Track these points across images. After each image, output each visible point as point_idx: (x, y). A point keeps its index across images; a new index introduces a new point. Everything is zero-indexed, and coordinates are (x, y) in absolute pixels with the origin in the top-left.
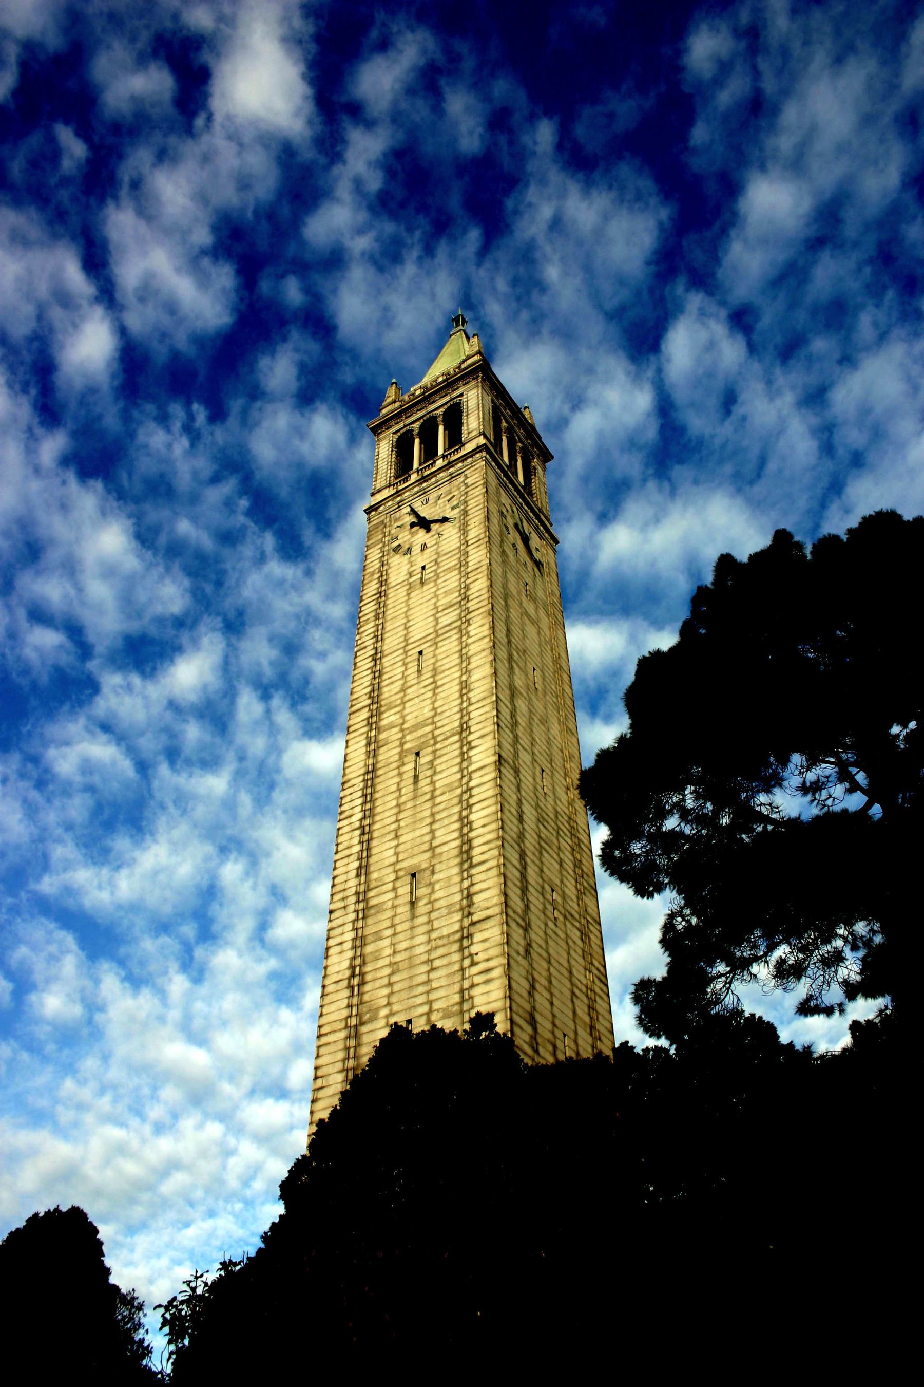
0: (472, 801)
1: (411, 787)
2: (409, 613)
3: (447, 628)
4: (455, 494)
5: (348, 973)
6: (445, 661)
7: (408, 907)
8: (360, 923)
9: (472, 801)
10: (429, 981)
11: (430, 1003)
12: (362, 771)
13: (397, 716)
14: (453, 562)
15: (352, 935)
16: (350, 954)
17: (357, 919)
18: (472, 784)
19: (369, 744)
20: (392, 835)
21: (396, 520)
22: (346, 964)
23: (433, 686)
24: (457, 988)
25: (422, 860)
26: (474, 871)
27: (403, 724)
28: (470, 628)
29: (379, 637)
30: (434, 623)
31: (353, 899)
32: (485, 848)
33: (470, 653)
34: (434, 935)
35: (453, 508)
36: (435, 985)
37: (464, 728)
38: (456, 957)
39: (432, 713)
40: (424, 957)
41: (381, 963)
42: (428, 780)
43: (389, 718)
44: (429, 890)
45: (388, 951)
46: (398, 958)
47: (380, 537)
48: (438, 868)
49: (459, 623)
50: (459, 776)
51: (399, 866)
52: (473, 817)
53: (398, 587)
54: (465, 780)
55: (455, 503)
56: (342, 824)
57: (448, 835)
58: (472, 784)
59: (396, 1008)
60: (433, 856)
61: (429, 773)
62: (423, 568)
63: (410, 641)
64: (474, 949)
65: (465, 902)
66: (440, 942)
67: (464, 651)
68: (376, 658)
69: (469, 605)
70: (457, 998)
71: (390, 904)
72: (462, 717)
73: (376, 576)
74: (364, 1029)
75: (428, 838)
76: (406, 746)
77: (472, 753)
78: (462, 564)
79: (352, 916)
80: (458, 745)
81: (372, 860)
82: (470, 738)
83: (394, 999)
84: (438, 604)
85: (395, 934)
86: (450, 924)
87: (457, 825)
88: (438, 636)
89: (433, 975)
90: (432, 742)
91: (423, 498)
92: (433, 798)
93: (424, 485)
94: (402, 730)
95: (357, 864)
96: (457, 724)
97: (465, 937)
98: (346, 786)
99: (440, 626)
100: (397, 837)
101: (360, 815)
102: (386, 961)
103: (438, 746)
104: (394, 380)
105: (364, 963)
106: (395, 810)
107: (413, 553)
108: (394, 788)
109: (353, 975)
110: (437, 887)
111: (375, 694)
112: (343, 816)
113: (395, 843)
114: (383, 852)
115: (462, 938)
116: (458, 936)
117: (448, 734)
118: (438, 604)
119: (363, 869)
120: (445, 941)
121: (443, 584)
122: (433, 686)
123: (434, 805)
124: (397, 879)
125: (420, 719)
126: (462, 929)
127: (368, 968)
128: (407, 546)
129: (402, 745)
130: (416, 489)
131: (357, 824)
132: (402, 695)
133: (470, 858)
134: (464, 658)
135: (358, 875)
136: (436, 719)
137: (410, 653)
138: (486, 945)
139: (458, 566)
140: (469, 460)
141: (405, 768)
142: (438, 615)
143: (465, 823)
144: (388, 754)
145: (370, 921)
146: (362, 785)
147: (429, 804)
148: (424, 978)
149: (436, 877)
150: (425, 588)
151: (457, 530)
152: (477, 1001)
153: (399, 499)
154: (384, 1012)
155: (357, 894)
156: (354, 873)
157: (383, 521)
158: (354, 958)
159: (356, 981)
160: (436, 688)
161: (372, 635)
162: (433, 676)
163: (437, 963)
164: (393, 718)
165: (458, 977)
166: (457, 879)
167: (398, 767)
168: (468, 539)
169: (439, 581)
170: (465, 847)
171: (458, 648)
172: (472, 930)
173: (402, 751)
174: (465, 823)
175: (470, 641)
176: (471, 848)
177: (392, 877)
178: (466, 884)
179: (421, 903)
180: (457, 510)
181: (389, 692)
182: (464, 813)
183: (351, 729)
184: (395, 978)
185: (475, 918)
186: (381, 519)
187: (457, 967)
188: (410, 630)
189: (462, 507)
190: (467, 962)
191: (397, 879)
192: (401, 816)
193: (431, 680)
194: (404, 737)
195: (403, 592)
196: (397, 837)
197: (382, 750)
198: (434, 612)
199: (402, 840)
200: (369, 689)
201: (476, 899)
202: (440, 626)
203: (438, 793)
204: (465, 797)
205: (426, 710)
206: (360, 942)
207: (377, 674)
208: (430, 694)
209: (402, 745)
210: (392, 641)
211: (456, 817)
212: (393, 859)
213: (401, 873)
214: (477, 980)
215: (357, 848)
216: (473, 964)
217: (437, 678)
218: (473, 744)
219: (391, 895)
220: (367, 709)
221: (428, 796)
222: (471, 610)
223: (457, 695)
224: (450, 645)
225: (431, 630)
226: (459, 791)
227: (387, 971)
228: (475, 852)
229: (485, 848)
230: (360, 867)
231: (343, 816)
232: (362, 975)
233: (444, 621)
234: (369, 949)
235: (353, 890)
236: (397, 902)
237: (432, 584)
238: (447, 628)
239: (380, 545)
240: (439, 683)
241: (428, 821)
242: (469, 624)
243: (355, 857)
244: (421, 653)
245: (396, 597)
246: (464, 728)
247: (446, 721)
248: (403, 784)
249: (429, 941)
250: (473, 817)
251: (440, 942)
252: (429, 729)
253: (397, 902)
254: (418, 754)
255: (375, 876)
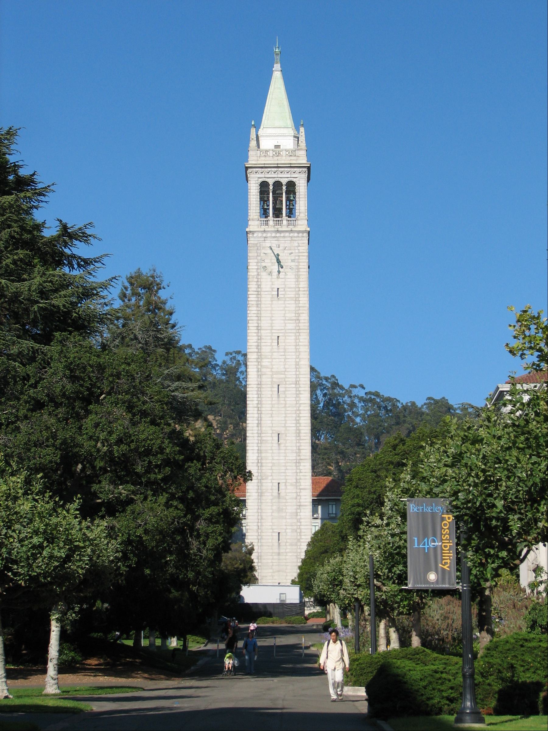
0: (301, 415)
1: (277, 399)
3: (290, 331)
4: (293, 252)
5: (256, 461)
6: (289, 347)
7: (277, 445)
8: (259, 445)
9: (301, 415)
10: (285, 473)
11: (286, 479)
12: (256, 383)
14: (292, 295)
15: (257, 448)
16: (257, 455)
17: (258, 443)
18: (301, 408)
19: (258, 371)
20: (270, 415)
21: (264, 248)
22: (256, 458)
24: (295, 477)
25: (282, 430)
26: (301, 441)
27: (272, 368)
28: (300, 337)
29: (259, 318)
31: (256, 435)
32: (305, 435)
33: (300, 350)
34: (287, 458)
35: (293, 261)
36: (287, 474)
37: (297, 383)
38: (295, 468)
39: (284, 370)
40: (284, 464)
41: (268, 461)
42: (283, 399)
43: (265, 362)
44: (284, 442)
45: (270, 458)
46: (274, 461)
47: (256, 254)
48: (288, 435)
49: (294, 331)
50: (295, 402)
51: (273, 429)
52: (301, 422)
53: (266, 293)
54: (298, 405)
55: (293, 258)
57: (291, 423)
58: (301, 408)
59: (274, 478)
60: (286, 430)
61: (284, 396)
62: (278, 289)
64: (301, 468)
65: (297, 451)
66: (289, 461)
67: (298, 347)
68: (258, 328)
69: (300, 325)
70: (295, 481)
71: (270, 442)
72: (296, 378)
73: (256, 280)
74: (263, 481)
75: (284, 422)
77: (301, 396)
78: (297, 299)
79: (257, 441)
80: (294, 389)
81: (262, 422)
82: (300, 389)
83: (273, 474)
84: (286, 315)
85: (272, 453)
86: (292, 456)
87: (295, 422)
89: (287, 471)
91: (277, 242)
92: (285, 407)
93: (278, 235)
95: (257, 422)
96: (294, 380)
97: (298, 462)
101: (257, 402)
102: (270, 461)
103: (287, 386)
104: (253, 123)
105: (262, 459)
106: (270, 406)
107: (273, 277)
108: (269, 396)
109: (258, 462)
110: (288, 442)
111: (258, 347)
114: (266, 421)
115: (296, 462)
116: (295, 461)
117: (291, 382)
118: (286, 315)
119: (259, 424)
120: (290, 461)
121: (288, 305)
123: (286, 410)
124: (273, 433)
126: (296, 459)
127: (263, 461)
128: (270, 270)
129: (272, 378)
130: (274, 235)
131: (256, 406)
133: (299, 436)
134: (297, 351)
135: (258, 426)
137: (274, 334)
138: (305, 468)
139: (295, 299)
140: (300, 235)
141: (274, 389)
142: (286, 322)
143: (298, 422)
144: (266, 379)
145: (263, 445)
146: (256, 389)
147: (283, 409)
148: (283, 471)
149: (287, 438)
150: (280, 302)
151: (293, 277)
152: (302, 484)
153: (264, 235)
154: (270, 478)
155: (257, 433)
156: (256, 425)
157: (256, 244)
158: (258, 456)
159: (259, 465)
161: (256, 315)
163: (288, 468)
165: (295, 474)
166: (295, 442)
167: (271, 388)
168: (300, 286)
170: (298, 431)
171: (295, 344)
172: (300, 461)
173: (272, 381)
174: (298, 422)
175: (300, 344)
176: (299, 433)
177: (271, 432)
178: (298, 445)
179: (282, 445)
180: (293, 264)
181: (266, 350)
182: (298, 418)
184: (273, 468)
185: (302, 458)
186: (256, 242)
187: (295, 471)
188: (274, 322)
189: (297, 264)
190: (298, 471)
191: (273, 433)
192: (273, 409)
193: (283, 354)
194: (272, 375)
197: (264, 376)
198: (283, 318)
199: (274, 419)
200: (256, 344)
201: (302, 451)
203: (287, 406)
204: (298, 412)
205: (282, 367)
206: (260, 451)
207: (260, 338)
208: (283, 360)
210: (265, 324)
211: (294, 419)
212: (271, 425)
213: (274, 432)
214: (302, 477)
215: (256, 415)
216: (300, 472)
217: (286, 354)
218: (301, 392)
219: (270, 438)
220: (256, 354)
221: (283, 406)
222: (301, 328)
223: (294, 366)
224: (291, 339)
226: (295, 409)
227: (270, 465)
228: (301, 435)
229: (305, 435)
230: (258, 424)
232: (261, 463)
234: (263, 455)
235: (256, 432)
236: (273, 442)
237: (282, 302)
238: (290, 331)
239: (256, 261)
241: (284, 415)
242: (300, 335)
244: (278, 337)
245: (266, 299)
246: (297, 383)
247: (290, 376)
248: (273, 396)
249: (285, 459)
250: (301, 422)
251: (289, 461)
252: (283, 376)
253: (273, 442)
254: (278, 385)
255: (264, 429)
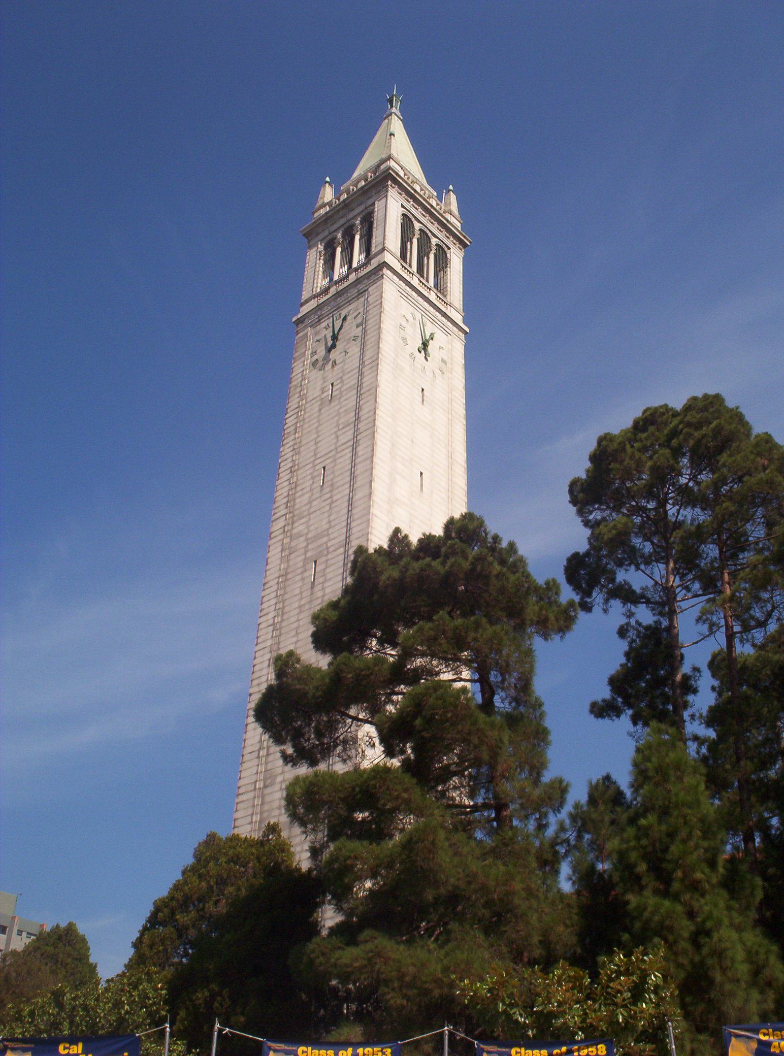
1: (309, 592)
2: (320, 428)
13: (304, 526)
20: (294, 633)
23: (329, 501)
27: (307, 534)
30: (335, 441)
39: (327, 526)
56: (261, 620)
62: (332, 384)
63: (318, 456)
76: (309, 554)
80: (342, 557)
88: (337, 453)
90: (325, 552)
94: (307, 540)
98: (267, 586)
99: (340, 443)
100: (297, 634)
103: (330, 556)
112: (263, 613)
113: (295, 639)
122: (329, 501)
125: (319, 530)
129: (305, 553)
132: (308, 506)
136: (330, 531)
142: (340, 432)
160: (332, 502)
162: (331, 491)
164: (301, 528)
167: (302, 573)
169: (342, 399)
173: (306, 559)
183: (273, 535)
188: (319, 444)
195: (316, 407)
196: (297, 634)
198: (336, 429)
202: (340, 443)
209: (305, 553)
225: (333, 447)
231: (263, 613)
233: (343, 439)
240: (335, 498)
243: (268, 650)
244: (324, 468)
254: (315, 562)
